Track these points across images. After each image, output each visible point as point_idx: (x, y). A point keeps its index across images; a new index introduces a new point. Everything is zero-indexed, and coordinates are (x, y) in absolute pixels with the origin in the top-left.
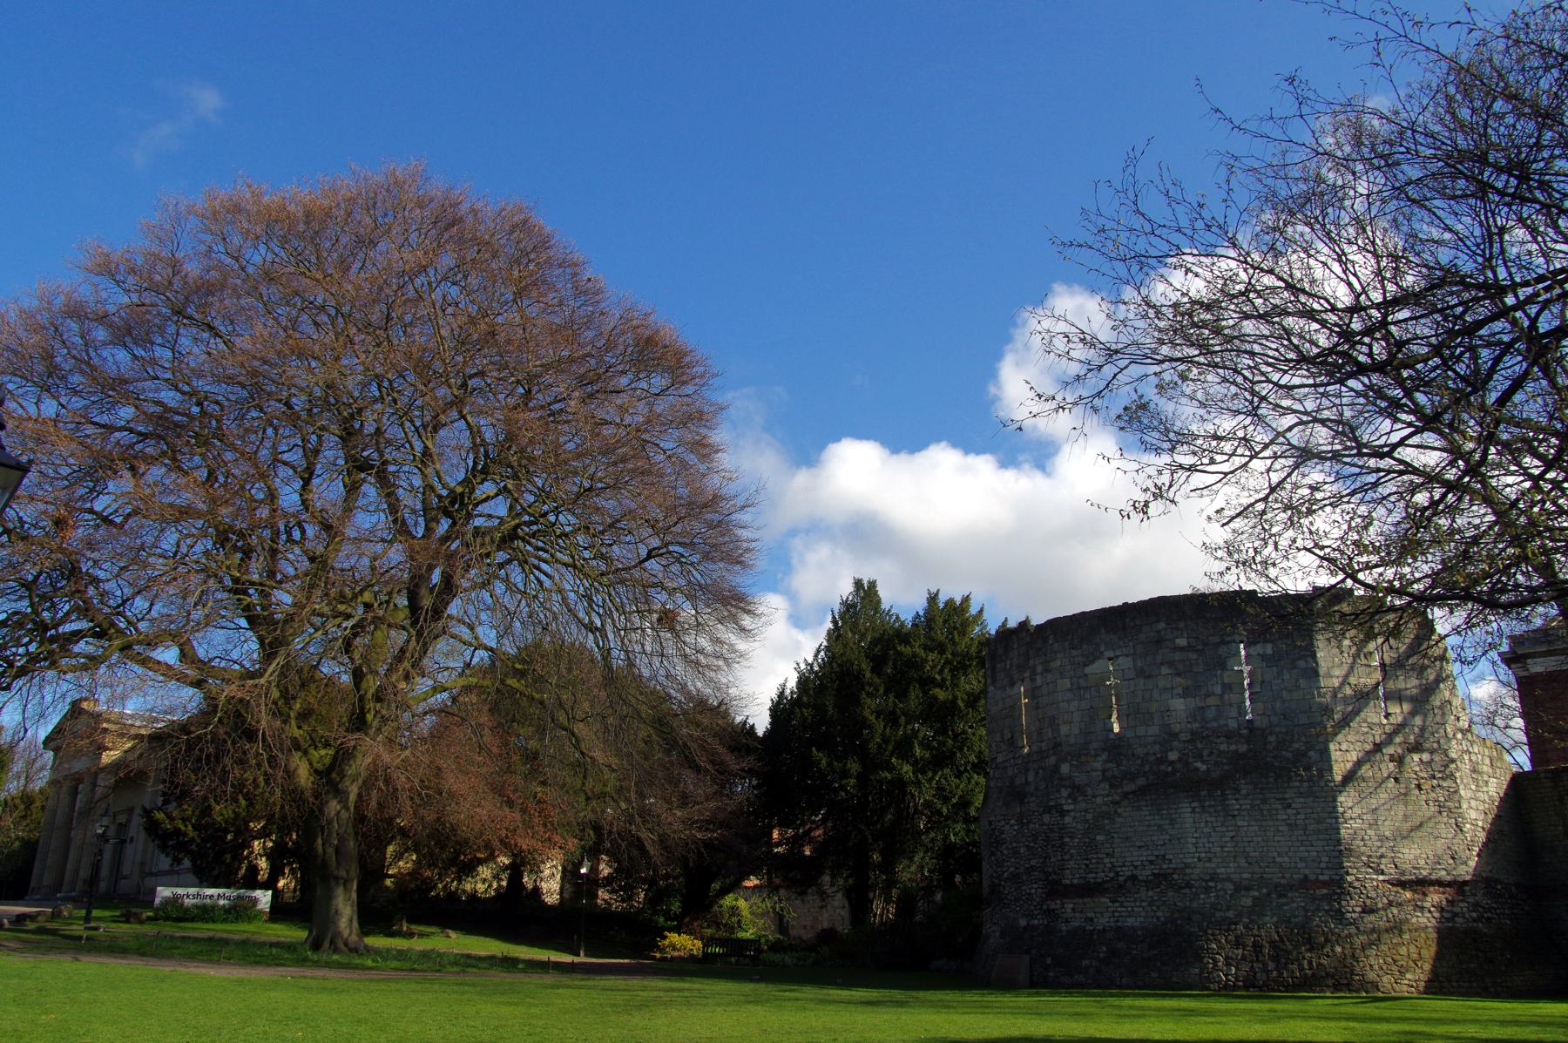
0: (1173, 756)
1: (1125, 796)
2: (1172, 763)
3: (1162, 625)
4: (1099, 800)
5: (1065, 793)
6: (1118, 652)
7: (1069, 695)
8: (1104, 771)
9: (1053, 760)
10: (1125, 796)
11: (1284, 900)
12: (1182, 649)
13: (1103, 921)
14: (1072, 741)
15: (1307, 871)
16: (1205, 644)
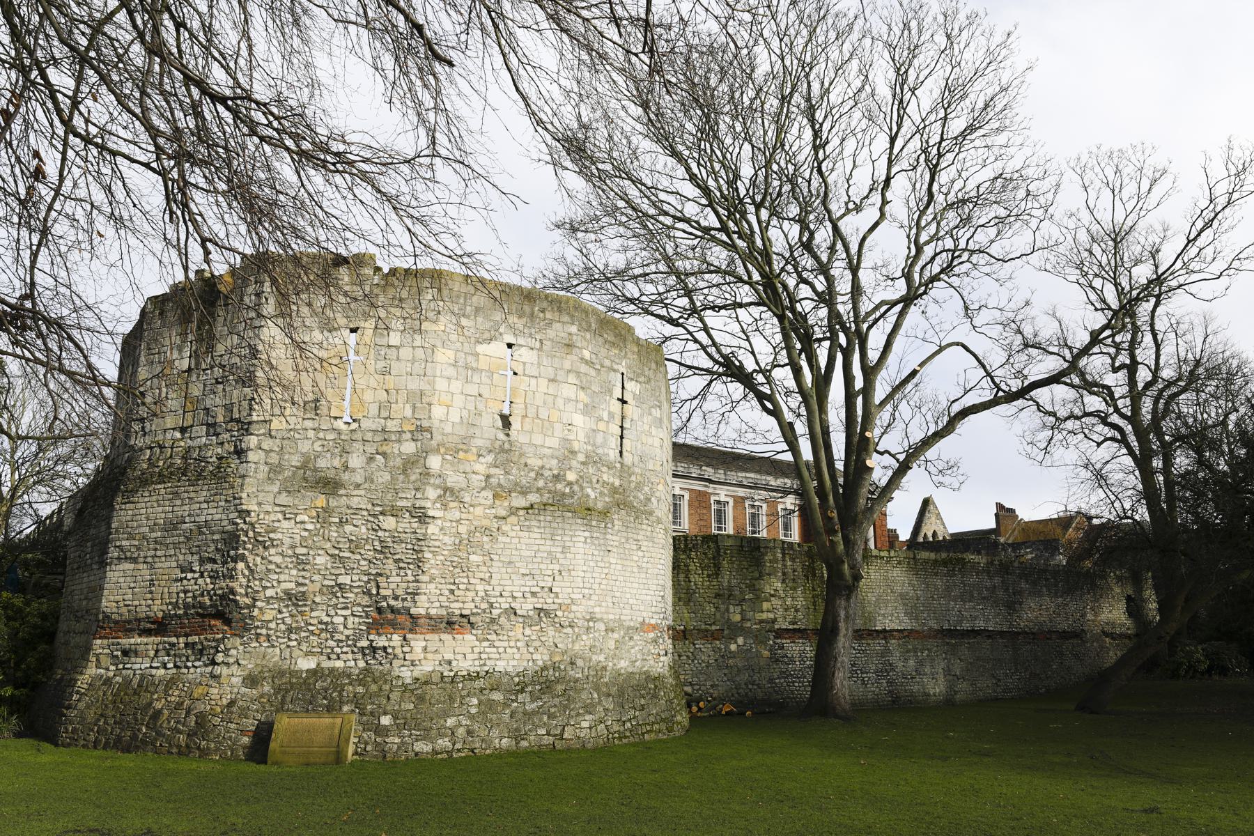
0: (571, 476)
1: (513, 511)
2: (570, 484)
3: (574, 329)
4: (479, 511)
5: (432, 493)
6: (521, 341)
7: (451, 372)
8: (488, 477)
9: (409, 448)
10: (513, 511)
11: (632, 643)
12: (586, 362)
13: (464, 665)
14: (448, 429)
15: (644, 614)
16: (602, 366)
